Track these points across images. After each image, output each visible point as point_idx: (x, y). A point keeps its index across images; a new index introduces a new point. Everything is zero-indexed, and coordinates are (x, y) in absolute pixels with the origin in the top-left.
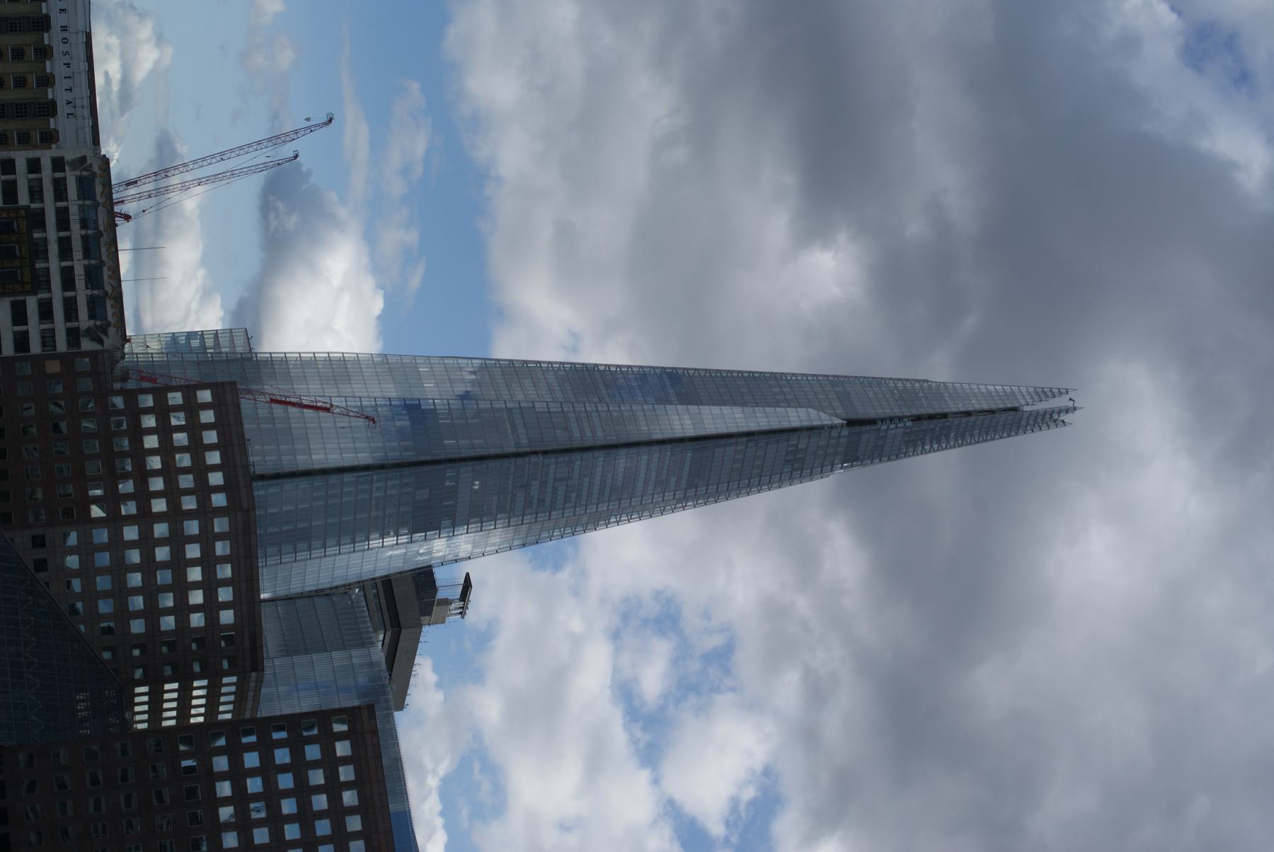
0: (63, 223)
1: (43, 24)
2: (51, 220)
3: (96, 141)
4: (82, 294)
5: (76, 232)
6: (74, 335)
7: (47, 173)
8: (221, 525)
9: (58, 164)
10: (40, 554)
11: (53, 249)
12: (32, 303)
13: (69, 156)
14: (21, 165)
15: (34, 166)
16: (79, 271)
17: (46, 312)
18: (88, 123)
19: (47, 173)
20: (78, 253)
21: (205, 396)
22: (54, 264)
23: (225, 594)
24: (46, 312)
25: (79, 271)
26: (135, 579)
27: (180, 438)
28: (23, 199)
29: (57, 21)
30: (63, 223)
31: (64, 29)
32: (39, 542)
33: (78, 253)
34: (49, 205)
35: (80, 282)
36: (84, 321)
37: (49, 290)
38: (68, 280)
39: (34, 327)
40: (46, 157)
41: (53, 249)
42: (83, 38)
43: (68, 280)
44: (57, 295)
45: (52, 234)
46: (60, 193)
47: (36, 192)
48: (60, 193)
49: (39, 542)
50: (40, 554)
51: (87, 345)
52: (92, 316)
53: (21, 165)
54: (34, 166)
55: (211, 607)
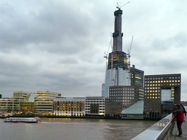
0: (92, 102)
3: (84, 98)
4: (99, 101)
5: (93, 101)
6: (103, 102)
7: (87, 103)
8: (124, 89)
9: (86, 102)
10: (125, 107)
11: (94, 103)
12: (100, 105)
13: (86, 101)
14: (86, 105)
15: (86, 104)
16: (97, 101)
18: (82, 99)
19: (87, 103)
20: (95, 101)
21: (111, 90)
22: (96, 103)
23: (131, 89)
25: (97, 101)
26: (156, 82)
27: (115, 92)
28: (90, 105)
30: (92, 102)
32: (124, 107)
33: (95, 101)
34: (90, 103)
35: (98, 101)
36: (102, 101)
38: (98, 102)
39: (102, 105)
40: (86, 103)
41: (94, 103)
42: (74, 99)
43: (98, 102)
45: (93, 103)
46: (89, 102)
48: (89, 102)
49: (124, 107)
50: (125, 107)
51: (104, 100)
52: (101, 100)
53: (86, 105)
54: (86, 104)
55: (132, 91)
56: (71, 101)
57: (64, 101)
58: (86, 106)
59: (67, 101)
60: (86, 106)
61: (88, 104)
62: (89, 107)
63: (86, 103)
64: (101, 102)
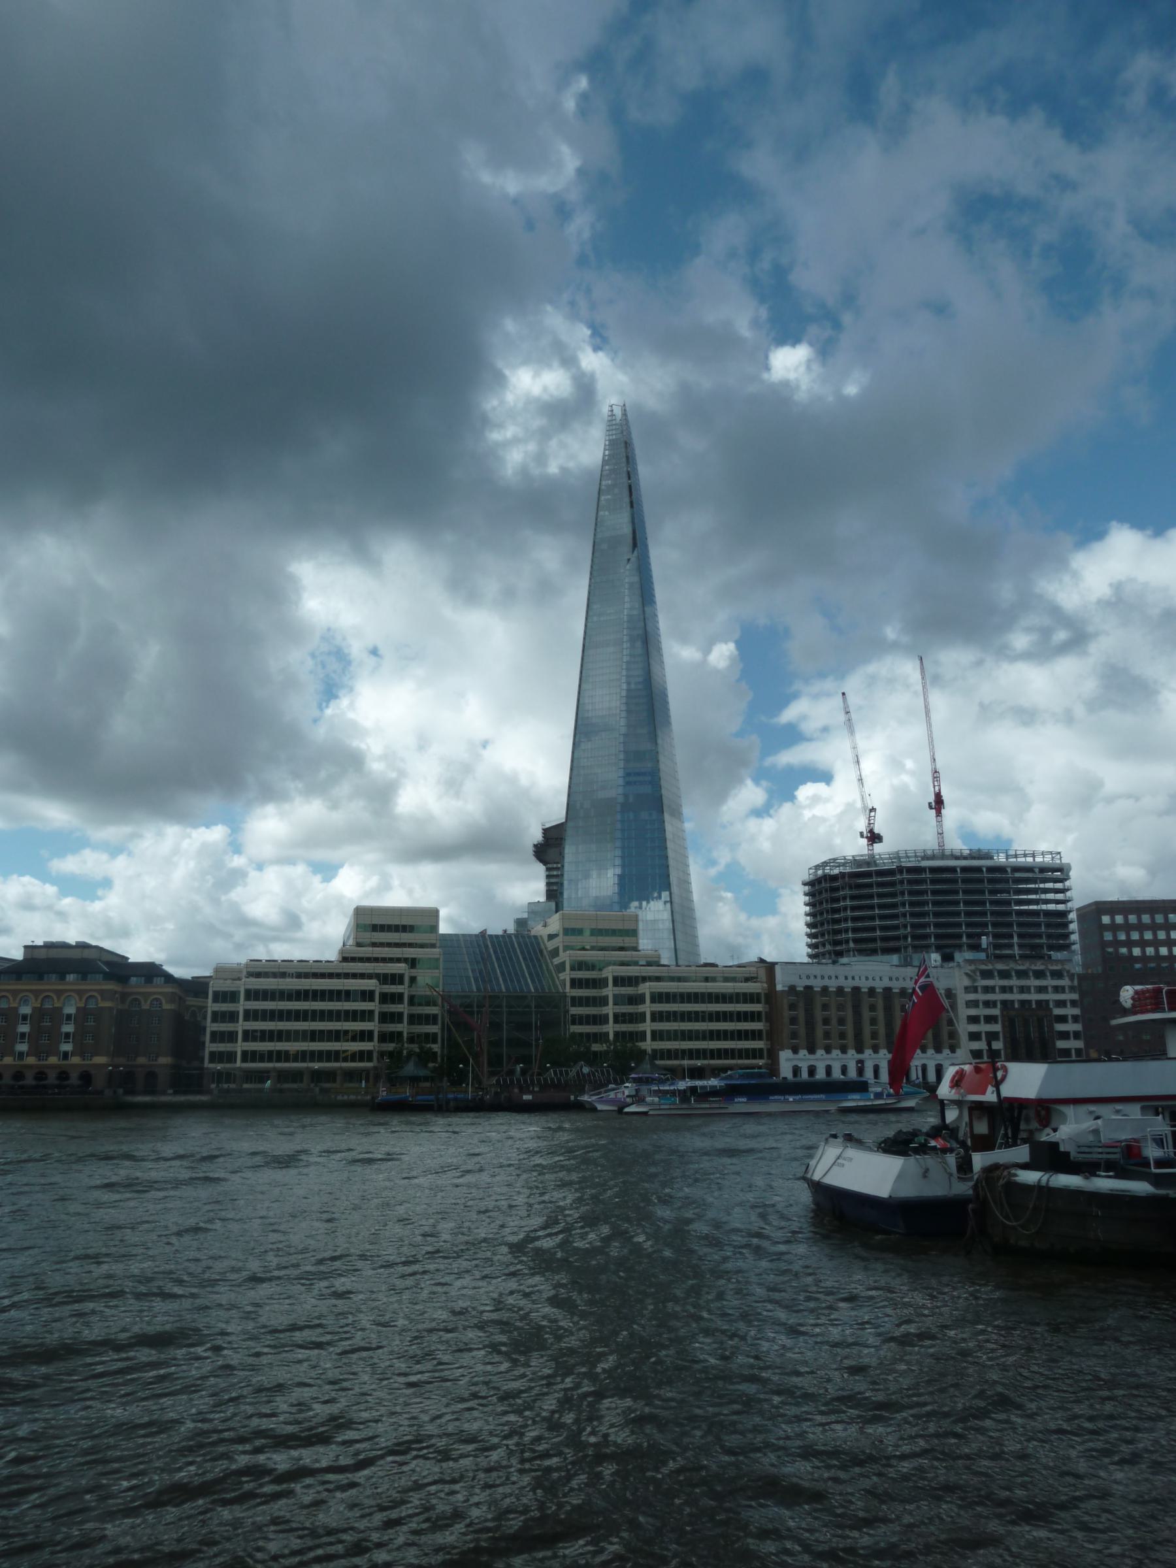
1: (888, 990)
2: (1007, 997)
12: (1058, 1011)
13: (967, 982)
17: (1061, 1004)
22: (1034, 997)
24: (1061, 1004)
29: (886, 983)
31: (891, 979)
34: (998, 997)
36: (1065, 982)
37: (1047, 1001)
38: (1042, 989)
43: (1042, 989)
44: (1051, 997)
45: (1016, 997)
47: (987, 1004)
56: (879, 986)
57: (841, 982)
58: (974, 1020)
59: (856, 983)
60: (974, 1020)
61: (987, 1004)
62: (990, 1019)
63: (972, 997)
64: (1057, 989)
